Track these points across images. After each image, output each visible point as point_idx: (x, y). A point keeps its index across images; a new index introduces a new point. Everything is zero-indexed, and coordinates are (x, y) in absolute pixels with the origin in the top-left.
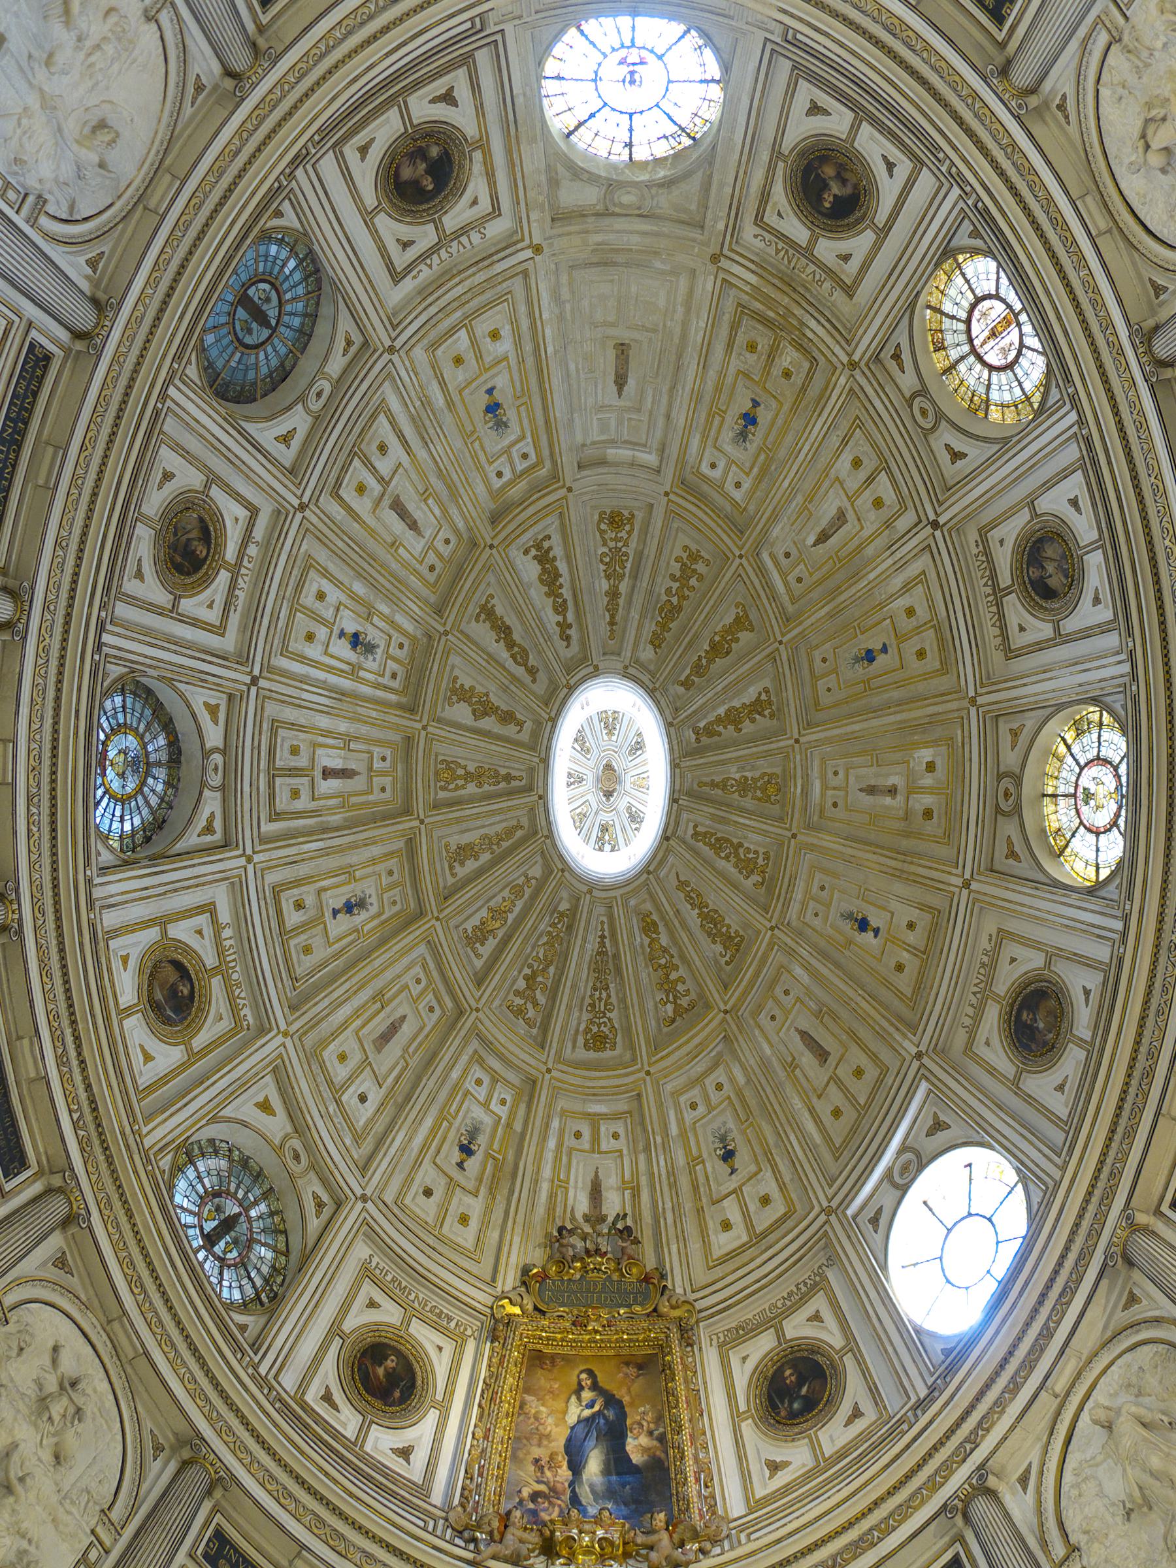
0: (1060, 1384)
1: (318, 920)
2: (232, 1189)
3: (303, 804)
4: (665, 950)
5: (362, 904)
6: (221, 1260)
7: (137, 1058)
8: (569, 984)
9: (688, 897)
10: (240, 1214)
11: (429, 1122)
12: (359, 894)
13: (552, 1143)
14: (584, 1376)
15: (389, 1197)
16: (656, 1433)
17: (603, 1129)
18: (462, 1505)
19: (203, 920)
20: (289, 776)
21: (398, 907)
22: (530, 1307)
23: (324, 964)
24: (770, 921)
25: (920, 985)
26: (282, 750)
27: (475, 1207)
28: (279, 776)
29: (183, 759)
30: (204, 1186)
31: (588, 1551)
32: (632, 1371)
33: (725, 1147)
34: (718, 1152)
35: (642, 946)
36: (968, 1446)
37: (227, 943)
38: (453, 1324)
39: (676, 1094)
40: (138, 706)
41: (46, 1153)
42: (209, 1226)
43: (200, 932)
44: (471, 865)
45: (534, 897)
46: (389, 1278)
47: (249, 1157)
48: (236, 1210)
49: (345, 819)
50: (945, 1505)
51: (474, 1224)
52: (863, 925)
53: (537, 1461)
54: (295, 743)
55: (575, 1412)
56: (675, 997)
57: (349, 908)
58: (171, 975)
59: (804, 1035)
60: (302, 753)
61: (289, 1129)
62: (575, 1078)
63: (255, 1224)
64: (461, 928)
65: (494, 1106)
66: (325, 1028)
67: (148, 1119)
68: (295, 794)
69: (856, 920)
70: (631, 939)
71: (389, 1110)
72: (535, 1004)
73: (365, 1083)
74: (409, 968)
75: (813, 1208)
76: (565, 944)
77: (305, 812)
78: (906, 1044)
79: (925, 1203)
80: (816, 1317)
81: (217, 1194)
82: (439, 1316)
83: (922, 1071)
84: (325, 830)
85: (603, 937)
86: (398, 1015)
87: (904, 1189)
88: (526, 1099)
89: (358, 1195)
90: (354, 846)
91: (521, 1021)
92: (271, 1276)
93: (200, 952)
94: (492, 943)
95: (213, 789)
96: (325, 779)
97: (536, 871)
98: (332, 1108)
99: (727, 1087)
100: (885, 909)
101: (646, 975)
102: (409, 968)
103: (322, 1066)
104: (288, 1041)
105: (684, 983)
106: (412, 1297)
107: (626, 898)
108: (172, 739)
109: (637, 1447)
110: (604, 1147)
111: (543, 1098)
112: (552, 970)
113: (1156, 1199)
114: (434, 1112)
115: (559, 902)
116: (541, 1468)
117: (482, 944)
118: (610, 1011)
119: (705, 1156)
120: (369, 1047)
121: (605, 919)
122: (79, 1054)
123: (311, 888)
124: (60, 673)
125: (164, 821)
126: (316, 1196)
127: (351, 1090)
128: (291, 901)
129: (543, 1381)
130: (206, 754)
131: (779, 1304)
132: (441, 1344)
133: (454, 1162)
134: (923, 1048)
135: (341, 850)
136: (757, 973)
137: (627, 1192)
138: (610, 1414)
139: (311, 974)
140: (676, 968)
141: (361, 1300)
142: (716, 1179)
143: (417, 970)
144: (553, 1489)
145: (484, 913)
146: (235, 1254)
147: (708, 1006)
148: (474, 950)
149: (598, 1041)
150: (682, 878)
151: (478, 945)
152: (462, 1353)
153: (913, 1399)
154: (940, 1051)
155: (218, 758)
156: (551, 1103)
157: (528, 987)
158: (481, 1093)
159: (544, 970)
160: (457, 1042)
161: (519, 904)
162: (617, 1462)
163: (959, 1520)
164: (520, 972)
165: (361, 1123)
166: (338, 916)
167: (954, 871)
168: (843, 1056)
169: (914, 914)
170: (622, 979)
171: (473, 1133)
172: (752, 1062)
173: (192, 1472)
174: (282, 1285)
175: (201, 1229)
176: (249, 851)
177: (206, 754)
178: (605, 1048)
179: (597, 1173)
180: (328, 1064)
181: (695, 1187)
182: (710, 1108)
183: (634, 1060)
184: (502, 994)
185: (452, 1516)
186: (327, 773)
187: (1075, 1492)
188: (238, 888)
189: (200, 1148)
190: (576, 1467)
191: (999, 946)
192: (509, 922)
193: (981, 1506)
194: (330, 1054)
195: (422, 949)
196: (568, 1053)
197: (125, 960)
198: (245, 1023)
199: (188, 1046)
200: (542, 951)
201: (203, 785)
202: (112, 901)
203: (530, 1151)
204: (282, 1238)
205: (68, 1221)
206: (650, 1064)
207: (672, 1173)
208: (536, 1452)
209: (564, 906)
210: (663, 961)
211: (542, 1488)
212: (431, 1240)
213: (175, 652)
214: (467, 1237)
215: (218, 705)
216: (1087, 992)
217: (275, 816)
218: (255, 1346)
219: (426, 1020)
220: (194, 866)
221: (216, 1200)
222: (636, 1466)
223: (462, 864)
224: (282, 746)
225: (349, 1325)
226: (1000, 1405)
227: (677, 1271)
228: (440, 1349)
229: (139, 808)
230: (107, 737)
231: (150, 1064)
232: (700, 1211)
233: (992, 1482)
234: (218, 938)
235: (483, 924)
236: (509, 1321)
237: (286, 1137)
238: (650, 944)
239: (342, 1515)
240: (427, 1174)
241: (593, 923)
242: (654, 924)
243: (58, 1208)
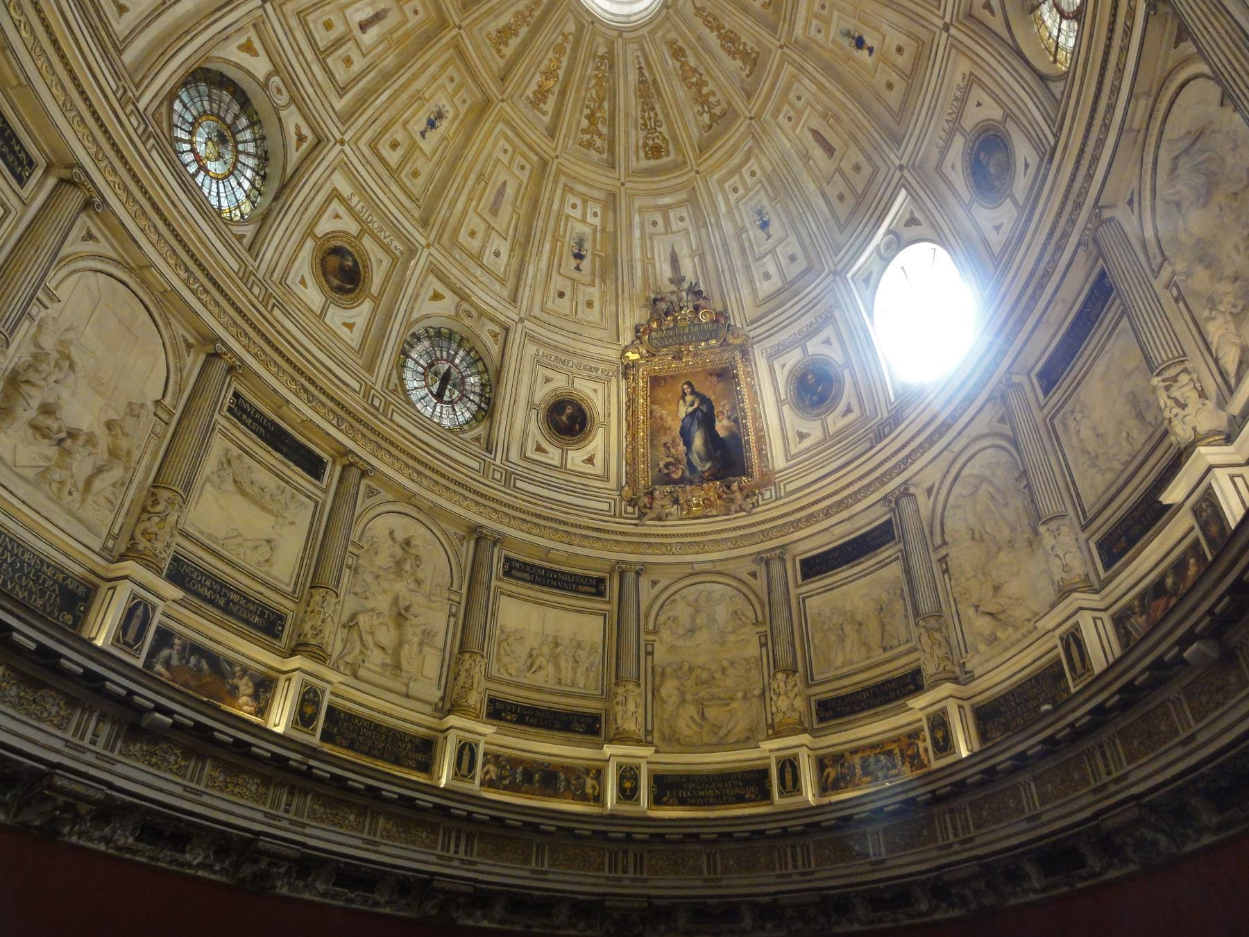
0: (957, 447)
1: (413, 146)
2: (439, 356)
3: (359, 64)
4: (694, 70)
5: (440, 116)
6: (451, 402)
7: (344, 333)
8: (622, 114)
9: (707, 23)
10: (449, 370)
11: (547, 247)
12: (435, 109)
13: (637, 233)
14: (685, 386)
15: (536, 311)
16: (732, 418)
17: (671, 215)
18: (627, 483)
19: (335, 205)
20: (336, 50)
21: (469, 102)
22: (644, 352)
23: (431, 177)
24: (779, 40)
25: (904, 102)
26: (318, 33)
27: (594, 292)
28: (328, 55)
29: (249, 95)
30: (422, 366)
31: (698, 505)
32: (714, 379)
33: (761, 219)
34: (757, 223)
35: (675, 69)
36: (902, 466)
37: (359, 207)
38: (600, 372)
39: (721, 182)
40: (193, 92)
42: (435, 390)
43: (337, 216)
44: (514, 42)
45: (575, 49)
46: (553, 358)
47: (440, 328)
48: (446, 367)
49: (398, 56)
50: (885, 497)
51: (597, 304)
52: (860, 43)
53: (665, 444)
54: (325, 18)
55: (683, 410)
56: (709, 108)
57: (431, 124)
58: (334, 261)
59: (815, 133)
60: (335, 23)
61: (457, 299)
62: (644, 184)
63: (461, 367)
64: (524, 98)
65: (590, 219)
66: (453, 222)
67: (370, 369)
68: (348, 61)
69: (853, 38)
70: (665, 67)
71: (517, 252)
72: (600, 135)
73: (497, 243)
74: (495, 145)
75: (824, 270)
76: (611, 80)
77: (362, 72)
78: (892, 156)
79: (903, 268)
80: (827, 342)
81: (431, 365)
82: (590, 370)
83: (903, 181)
84: (387, 76)
85: (640, 68)
86: (499, 184)
87: (887, 261)
88: (611, 206)
89: (517, 320)
90: (414, 78)
91: (593, 151)
92: (482, 390)
93: (344, 228)
94: (552, 100)
95: (286, 106)
96: (364, 33)
97: (570, 28)
98: (479, 272)
99: (759, 173)
100: (878, 31)
101: (682, 93)
102: (495, 145)
103: (462, 248)
104: (432, 250)
105: (714, 95)
106: (570, 364)
107: (652, 33)
108: (231, 89)
109: (722, 426)
110: (674, 228)
111: (623, 206)
112: (606, 105)
113: (1029, 366)
114: (549, 238)
115: (598, 46)
116: (668, 448)
117: (545, 103)
118: (660, 126)
119: (748, 226)
120: (488, 217)
121: (639, 53)
122: (316, 386)
123: (398, 126)
124: (142, 187)
125: (266, 152)
126: (490, 331)
127: (487, 252)
128: (387, 147)
129: (661, 394)
130: (265, 86)
131: (804, 330)
132: (595, 387)
133: (572, 268)
134: (904, 162)
135: (404, 87)
136: (773, 87)
137: (696, 259)
138: (704, 408)
139: (426, 189)
140: (705, 83)
141: (540, 379)
142: (757, 242)
143: (502, 142)
144: (676, 459)
145: (538, 78)
146: (457, 393)
147: (737, 116)
148: (540, 110)
149: (656, 152)
150: (698, 5)
151: (541, 105)
152: (609, 389)
153: (879, 417)
154: (917, 168)
155: (276, 80)
156: (629, 208)
157: (591, 123)
158: (577, 213)
159: (600, 107)
160: (549, 187)
161: (565, 60)
162: (712, 437)
163: (893, 505)
164: (581, 113)
165: (502, 270)
166: (427, 135)
167: (936, 11)
168: (845, 152)
169: (902, 40)
170: (663, 99)
171: (580, 243)
172: (776, 157)
173: (483, 543)
174: (491, 391)
175: (431, 392)
176: (338, 136)
177: (265, 86)
178: (661, 156)
179: (673, 247)
180: (465, 244)
181: (743, 250)
182: (747, 190)
183: (685, 163)
184: (572, 135)
185: (623, 493)
186: (364, 26)
187: (952, 512)
188: (344, 166)
189: (409, 344)
190: (688, 443)
191: (967, 90)
192: (561, 77)
193: (904, 502)
194: (463, 237)
195: (501, 126)
196: (634, 164)
197: (303, 282)
198: (398, 253)
199: (370, 296)
200: (594, 92)
201: (276, 110)
202: (273, 263)
203: (622, 245)
204: (480, 364)
205: (364, 474)
206: (698, 165)
207: (725, 244)
208: (664, 439)
209: (602, 51)
210: (694, 80)
211: (671, 459)
212: (573, 327)
213: (192, 39)
214: (594, 314)
215: (249, 40)
216: (1027, 166)
217: (342, 91)
218: (489, 450)
219: (521, 177)
220: (307, 180)
221: (432, 369)
222: (722, 439)
223: (506, 44)
224: (316, 28)
225: (536, 401)
226: (921, 449)
227: (736, 313)
228: (595, 391)
229: (244, 164)
230: (191, 142)
231: (355, 329)
232: (748, 268)
233: (912, 490)
234: (350, 210)
235: (540, 87)
236: (634, 364)
237: (458, 306)
238: (681, 67)
239: (565, 523)
240: (558, 283)
241: (630, 59)
242: (681, 49)
243: (355, 473)
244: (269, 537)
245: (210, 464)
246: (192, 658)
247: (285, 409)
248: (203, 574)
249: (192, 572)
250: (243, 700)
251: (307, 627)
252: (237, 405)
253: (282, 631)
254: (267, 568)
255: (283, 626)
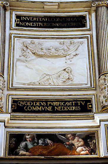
41: (84, 7)
244: (63, 69)
245: (17, 53)
246: (40, 141)
247: (45, 7)
248: (33, 101)
249: (26, 103)
250: (79, 149)
251: (102, 98)
252: (20, 21)
253: (92, 107)
254: (70, 82)
255: (92, 105)
